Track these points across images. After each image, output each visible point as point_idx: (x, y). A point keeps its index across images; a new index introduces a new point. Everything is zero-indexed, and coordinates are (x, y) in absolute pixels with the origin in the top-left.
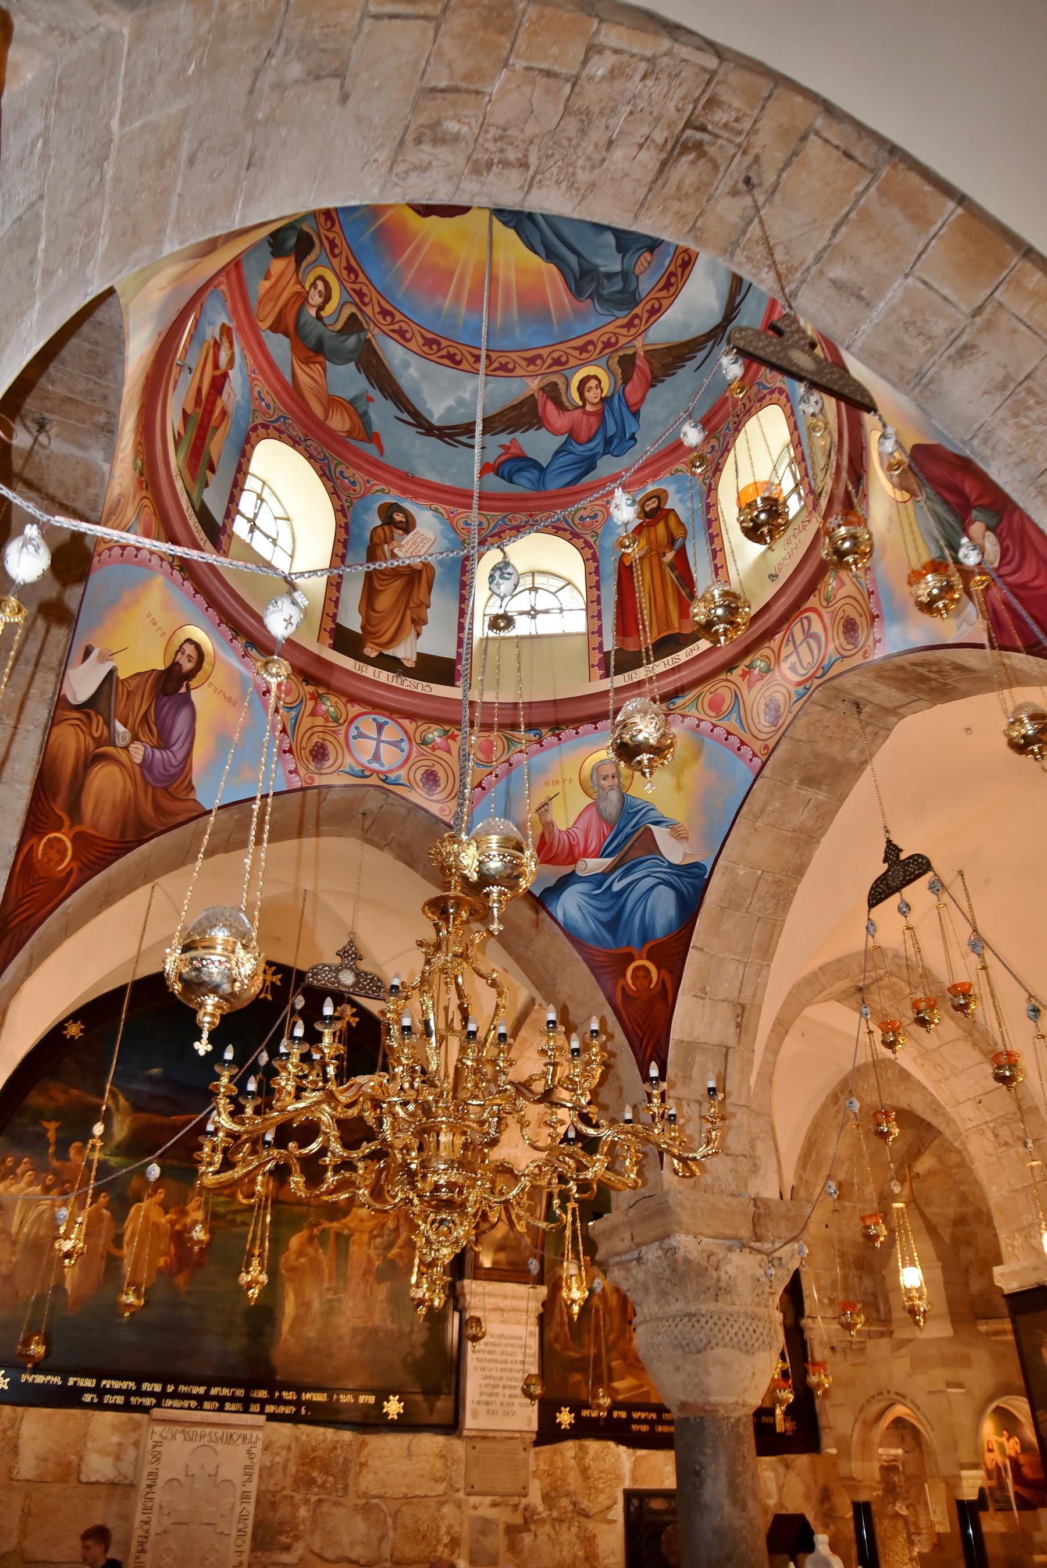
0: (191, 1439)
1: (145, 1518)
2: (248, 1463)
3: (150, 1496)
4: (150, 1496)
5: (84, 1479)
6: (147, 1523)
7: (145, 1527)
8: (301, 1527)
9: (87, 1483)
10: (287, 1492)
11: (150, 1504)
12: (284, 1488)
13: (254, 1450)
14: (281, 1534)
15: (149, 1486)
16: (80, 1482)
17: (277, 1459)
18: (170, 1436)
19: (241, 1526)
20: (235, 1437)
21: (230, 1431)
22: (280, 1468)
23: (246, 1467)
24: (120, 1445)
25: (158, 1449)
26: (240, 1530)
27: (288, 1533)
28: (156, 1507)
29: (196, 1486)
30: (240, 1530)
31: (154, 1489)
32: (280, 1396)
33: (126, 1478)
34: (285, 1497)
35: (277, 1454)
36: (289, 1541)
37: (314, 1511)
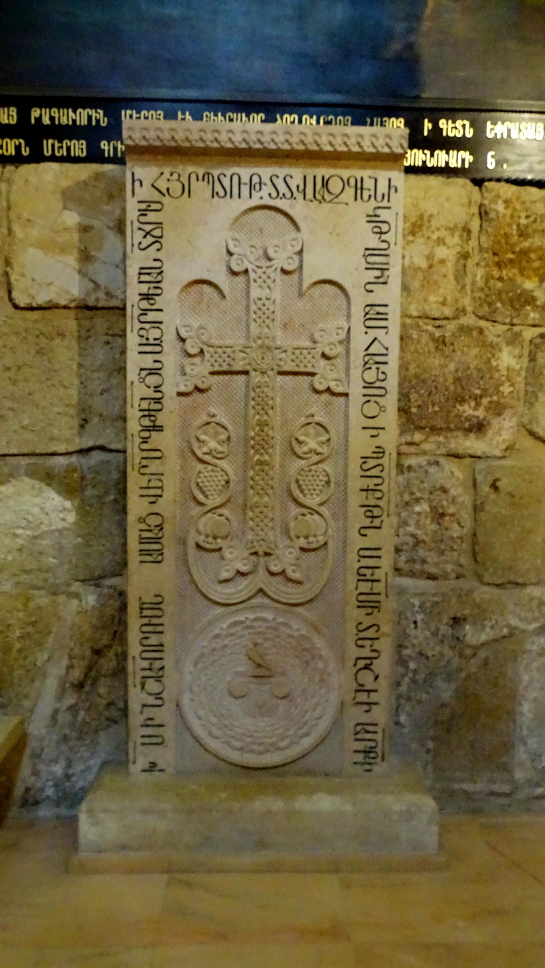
0: (228, 193)
1: (148, 361)
2: (374, 242)
3: (151, 316)
4: (151, 316)
5: (22, 300)
6: (153, 372)
7: (152, 380)
8: (506, 389)
9: (31, 308)
10: (469, 320)
11: (154, 333)
12: (461, 312)
13: (384, 215)
14: (462, 401)
15: (146, 297)
16: (16, 307)
17: (441, 252)
18: (176, 187)
19: (370, 376)
20: (335, 186)
21: (323, 172)
22: (450, 268)
23: (370, 252)
24: (85, 229)
25: (151, 217)
26: (369, 385)
27: (477, 399)
28: (169, 338)
29: (255, 293)
30: (369, 385)
31: (159, 302)
32: (437, 130)
33: (108, 294)
34: (465, 330)
35: (441, 241)
36: (480, 413)
37: (532, 358)
